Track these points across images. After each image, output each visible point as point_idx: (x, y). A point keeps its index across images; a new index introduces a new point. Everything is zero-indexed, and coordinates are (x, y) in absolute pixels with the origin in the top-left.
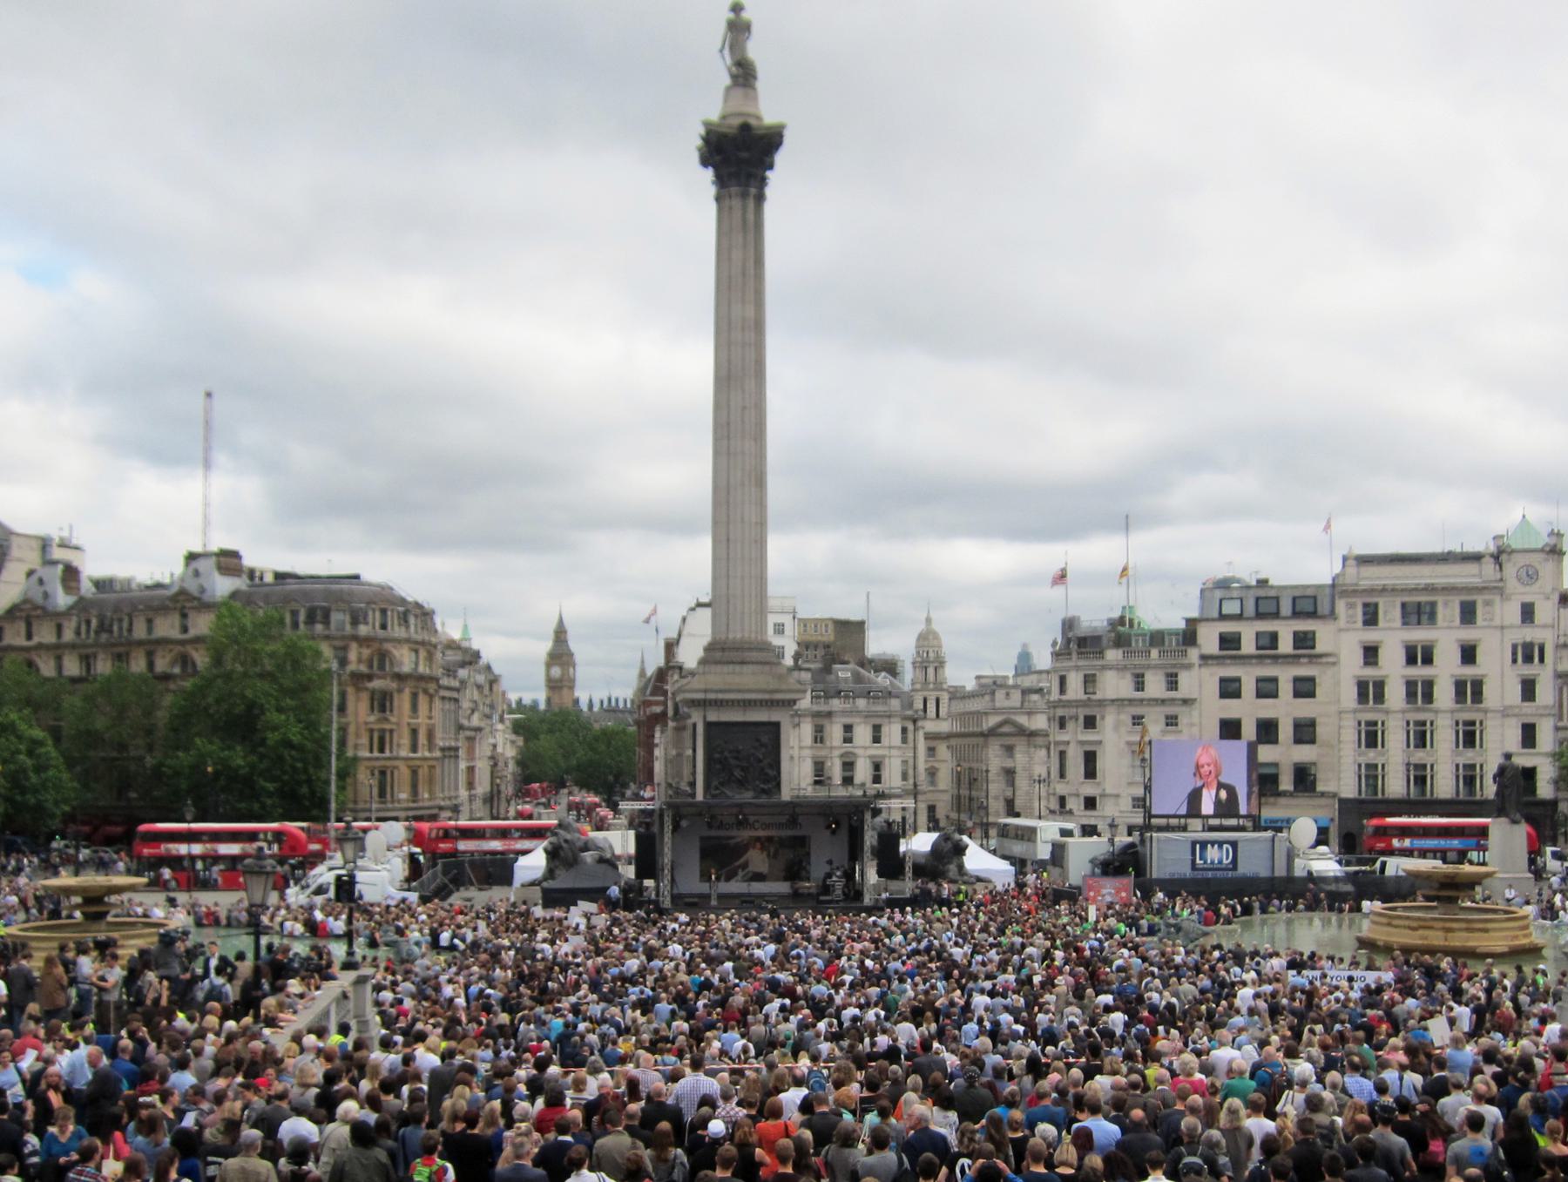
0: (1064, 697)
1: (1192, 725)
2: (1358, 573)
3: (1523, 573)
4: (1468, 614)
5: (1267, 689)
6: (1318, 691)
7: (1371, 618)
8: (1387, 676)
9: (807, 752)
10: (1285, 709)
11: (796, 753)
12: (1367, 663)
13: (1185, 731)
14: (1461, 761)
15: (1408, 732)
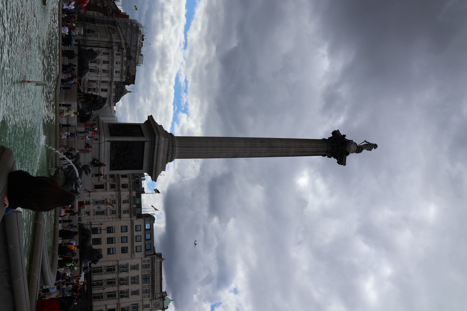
0: (120, 177)
1: (113, 218)
2: (158, 262)
3: (158, 304)
4: (146, 292)
5: (124, 240)
6: (123, 254)
7: (145, 267)
8: (128, 273)
9: (99, 79)
10: (118, 246)
11: (99, 75)
12: (131, 266)
13: (111, 217)
14: (104, 294)
15: (112, 279)
